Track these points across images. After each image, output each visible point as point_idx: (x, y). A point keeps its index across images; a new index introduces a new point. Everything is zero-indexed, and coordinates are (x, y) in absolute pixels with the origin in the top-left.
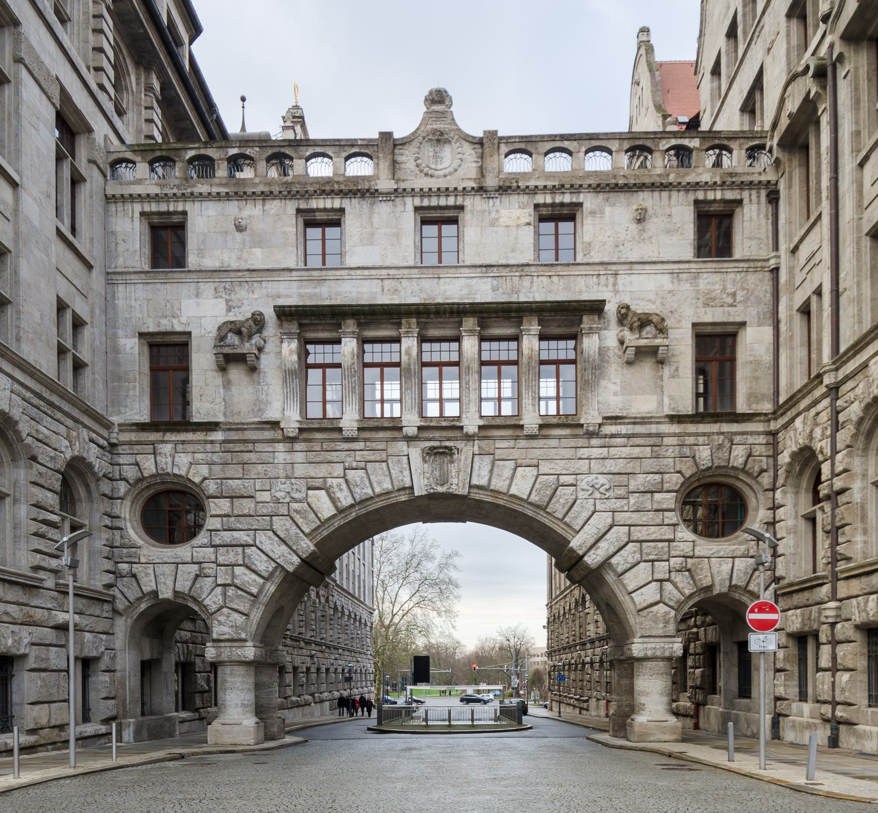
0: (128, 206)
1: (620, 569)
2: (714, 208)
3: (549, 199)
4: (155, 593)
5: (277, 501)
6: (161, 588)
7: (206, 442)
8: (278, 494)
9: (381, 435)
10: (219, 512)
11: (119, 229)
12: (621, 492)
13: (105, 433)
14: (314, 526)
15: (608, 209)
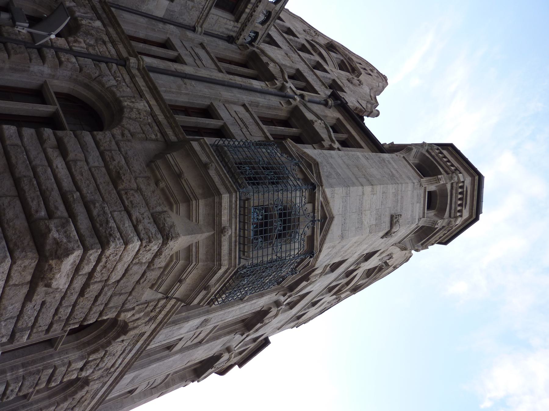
2: (242, 5)
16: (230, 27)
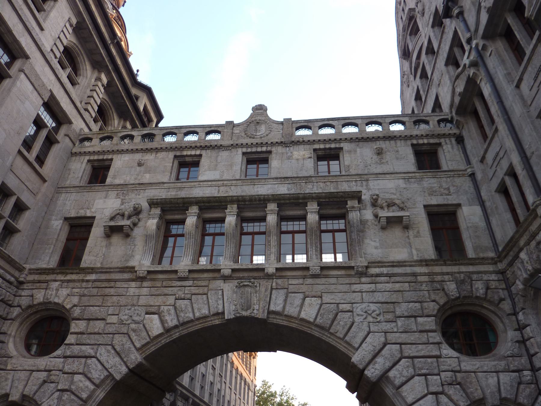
0: (82, 158)
1: (397, 382)
2: (424, 148)
3: (322, 146)
4: (7, 395)
5: (121, 322)
6: (14, 391)
7: (83, 281)
8: (123, 318)
9: (206, 275)
10: (77, 330)
11: (73, 167)
12: (390, 316)
13: (17, 274)
14: (144, 342)
15: (358, 150)
16: (449, 146)
